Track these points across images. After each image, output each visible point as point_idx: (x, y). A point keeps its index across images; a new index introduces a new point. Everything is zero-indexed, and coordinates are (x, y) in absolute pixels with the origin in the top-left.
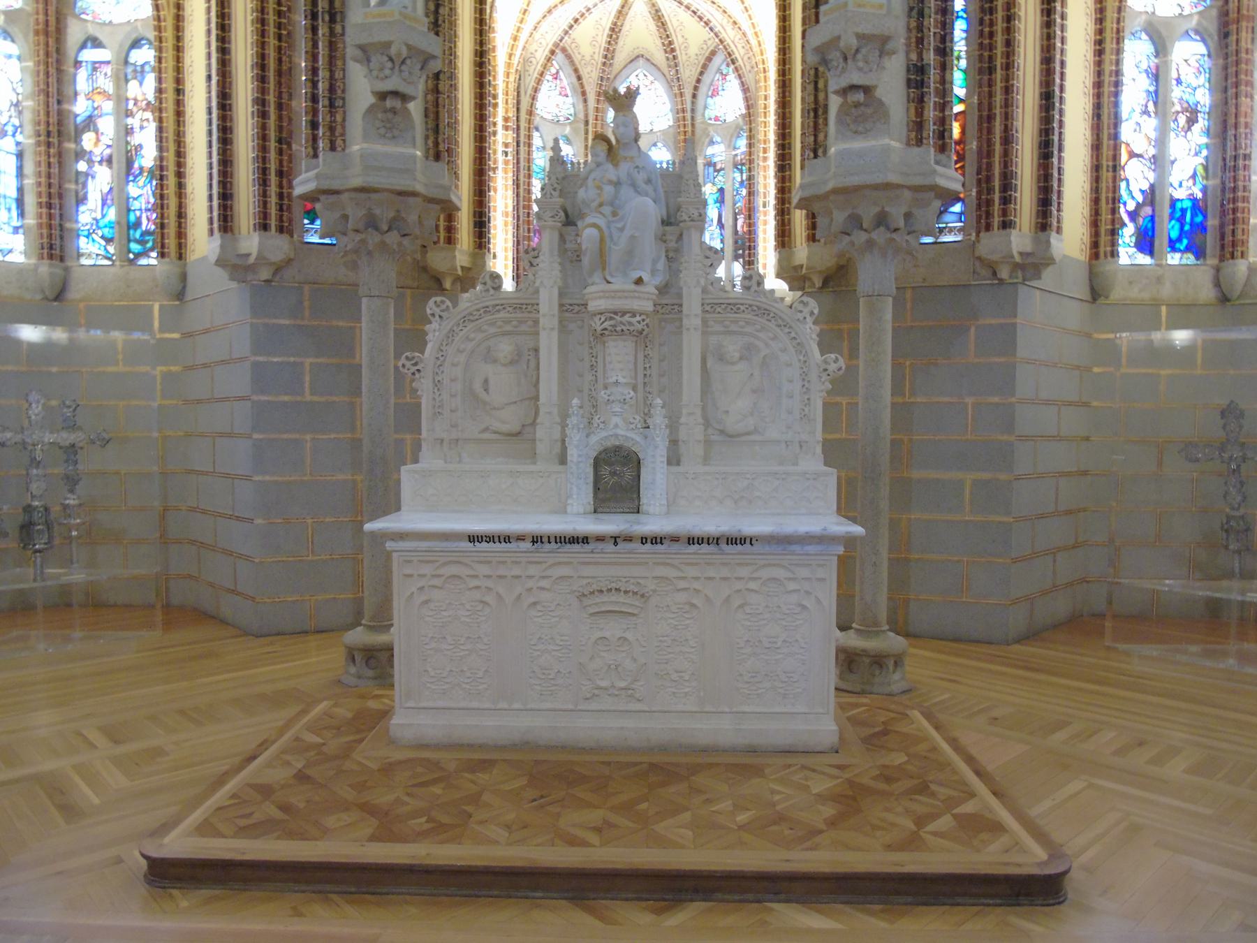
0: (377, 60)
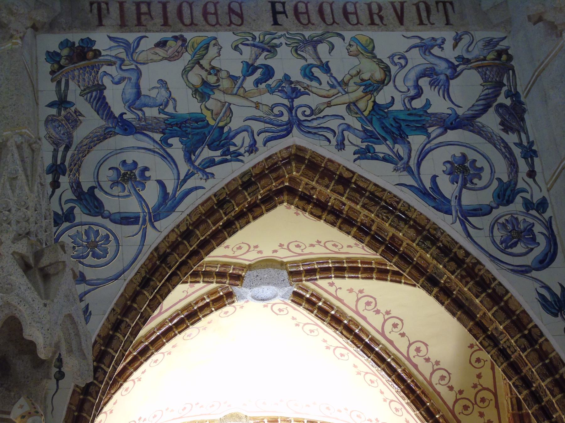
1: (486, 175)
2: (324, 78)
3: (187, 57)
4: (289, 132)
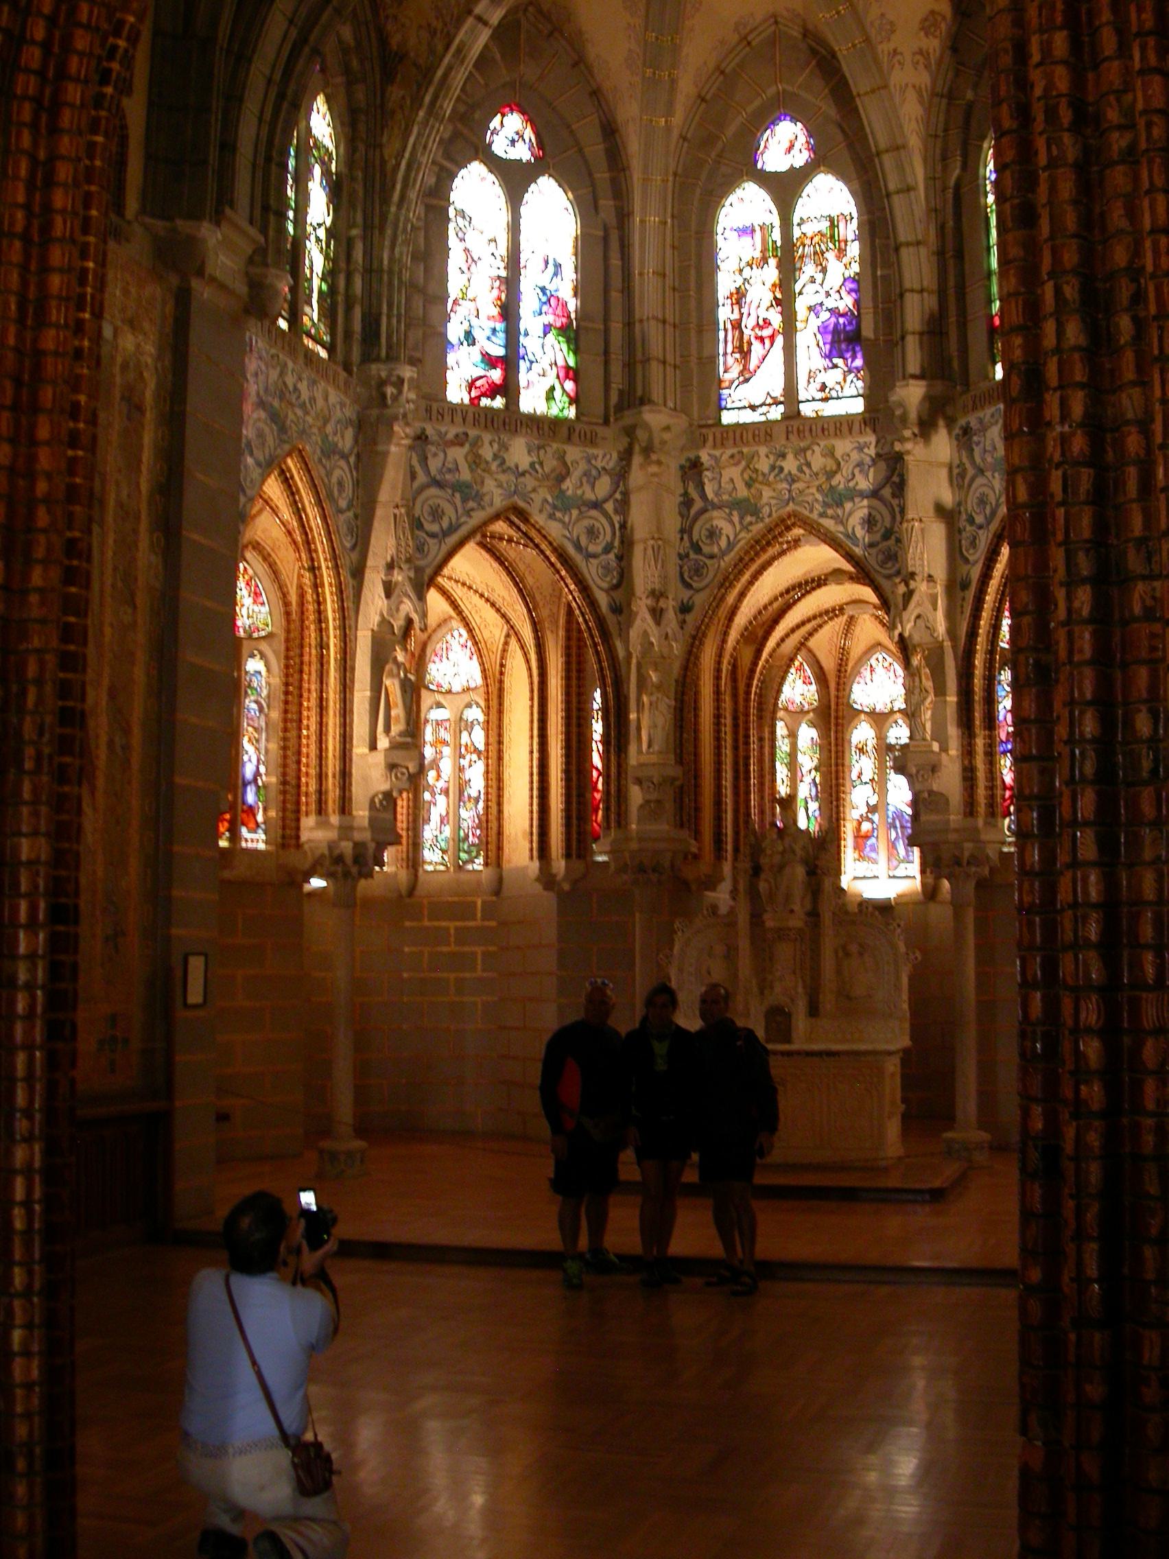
0: (645, 785)
1: (879, 525)
3: (744, 463)
4: (788, 504)
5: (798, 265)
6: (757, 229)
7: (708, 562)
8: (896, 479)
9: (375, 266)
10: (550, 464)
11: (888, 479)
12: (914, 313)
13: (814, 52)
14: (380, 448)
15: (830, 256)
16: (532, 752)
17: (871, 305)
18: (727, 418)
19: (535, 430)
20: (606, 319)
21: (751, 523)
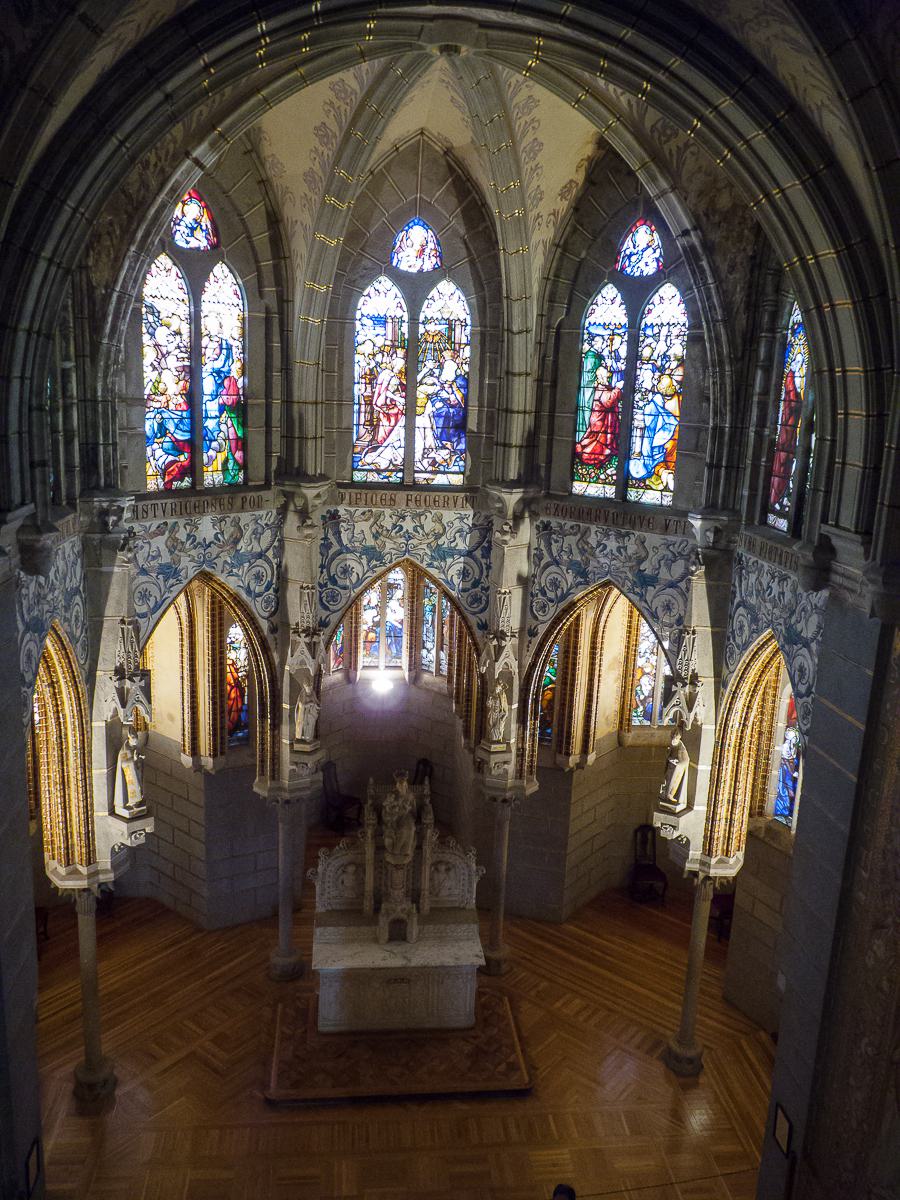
1: (471, 576)
2: (421, 531)
3: (372, 520)
5: (421, 358)
6: (389, 320)
7: (342, 591)
8: (485, 544)
9: (89, 396)
10: (229, 530)
11: (480, 544)
12: (518, 429)
13: (451, 169)
14: (104, 569)
15: (447, 354)
16: (182, 678)
17: (477, 404)
18: (358, 476)
19: (218, 507)
20: (268, 395)
21: (376, 566)
